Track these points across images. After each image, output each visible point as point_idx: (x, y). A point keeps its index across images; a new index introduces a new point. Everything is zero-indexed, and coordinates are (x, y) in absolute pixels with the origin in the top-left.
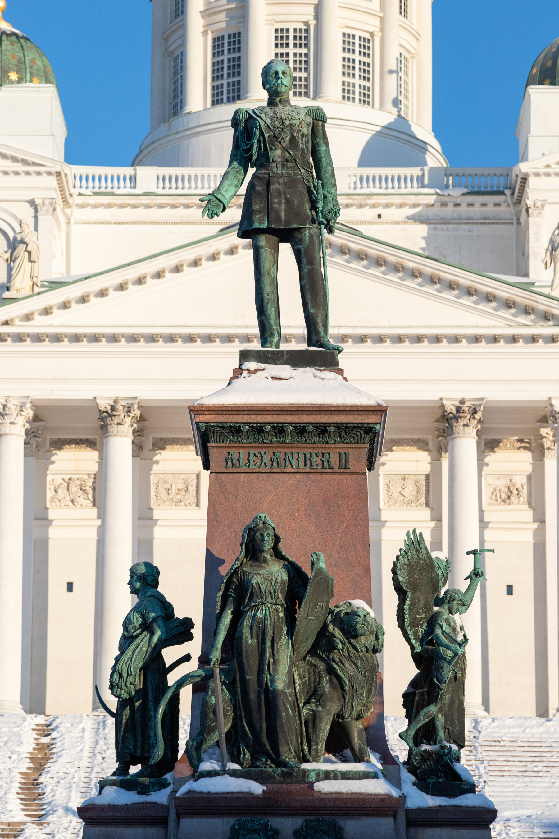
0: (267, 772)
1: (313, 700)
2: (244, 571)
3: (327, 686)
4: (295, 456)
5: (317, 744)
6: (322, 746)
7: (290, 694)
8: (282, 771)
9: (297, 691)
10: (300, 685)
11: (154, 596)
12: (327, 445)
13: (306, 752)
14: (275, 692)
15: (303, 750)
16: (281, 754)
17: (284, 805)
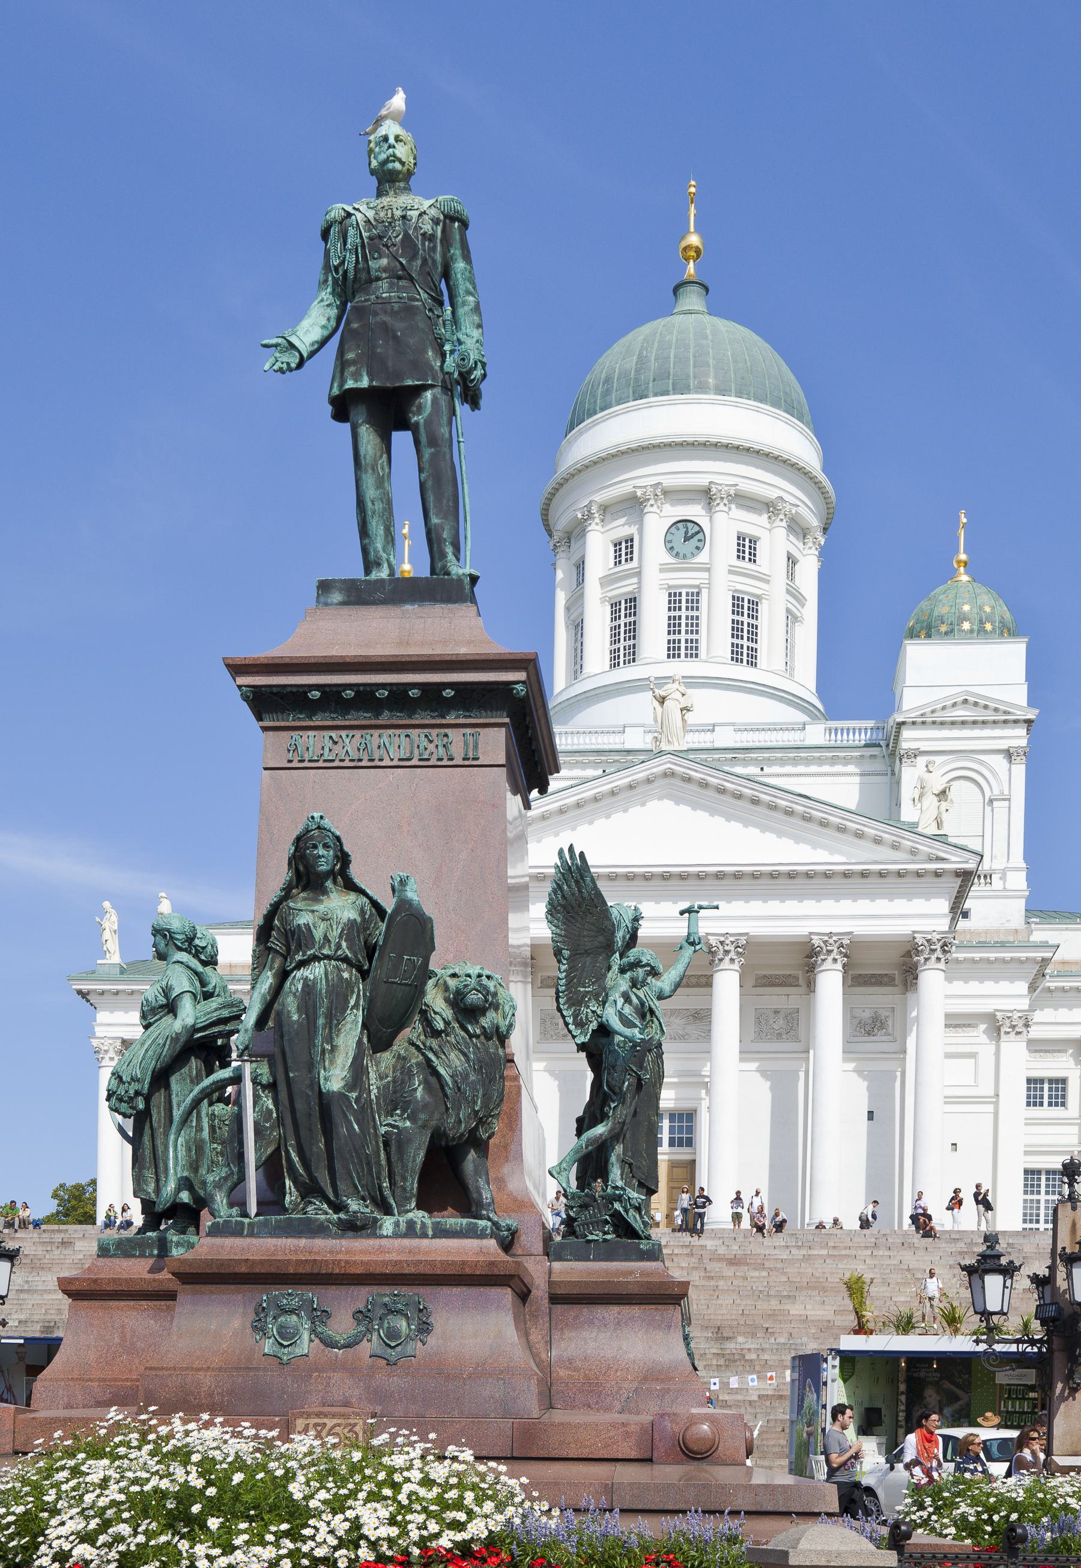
0: (317, 1220)
1: (398, 1112)
2: (290, 908)
3: (420, 1089)
5: (404, 1179)
6: (413, 1183)
7: (357, 1100)
8: (339, 1219)
9: (373, 1097)
10: (378, 1088)
11: (182, 963)
13: (387, 1193)
15: (380, 1188)
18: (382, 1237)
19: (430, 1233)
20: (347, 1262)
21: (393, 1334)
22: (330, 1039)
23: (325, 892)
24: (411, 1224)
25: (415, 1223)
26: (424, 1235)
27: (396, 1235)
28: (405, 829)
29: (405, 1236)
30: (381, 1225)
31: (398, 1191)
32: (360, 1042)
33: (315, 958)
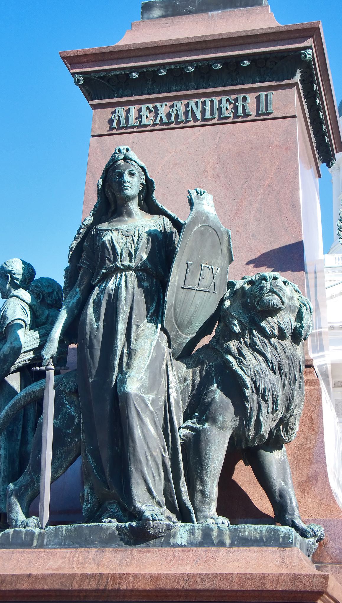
4: (200, 105)
7: (153, 402)
8: (131, 526)
9: (172, 400)
12: (242, 87)
13: (186, 497)
14: (126, 396)
16: (136, 498)
17: (124, 587)
18: (175, 546)
19: (228, 541)
20: (135, 576)
25: (211, 530)
26: (221, 544)
27: (192, 544)
28: (210, 174)
29: (201, 544)
30: (175, 533)
31: (198, 496)
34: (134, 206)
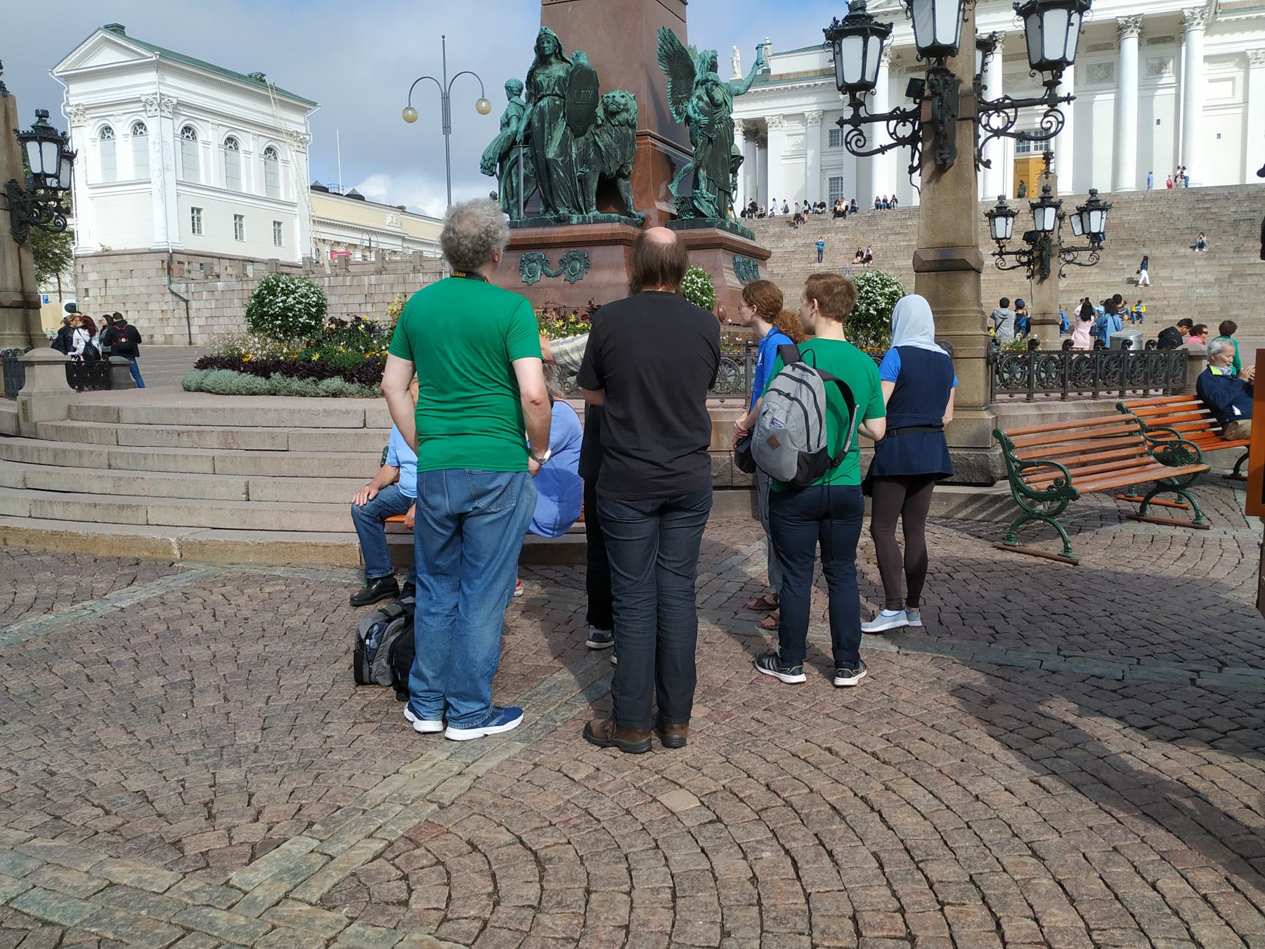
13: (582, 204)
21: (573, 269)
22: (550, 134)
23: (551, 64)
24: (584, 218)
27: (578, 223)
32: (565, 133)
33: (544, 96)
34: (553, 59)
